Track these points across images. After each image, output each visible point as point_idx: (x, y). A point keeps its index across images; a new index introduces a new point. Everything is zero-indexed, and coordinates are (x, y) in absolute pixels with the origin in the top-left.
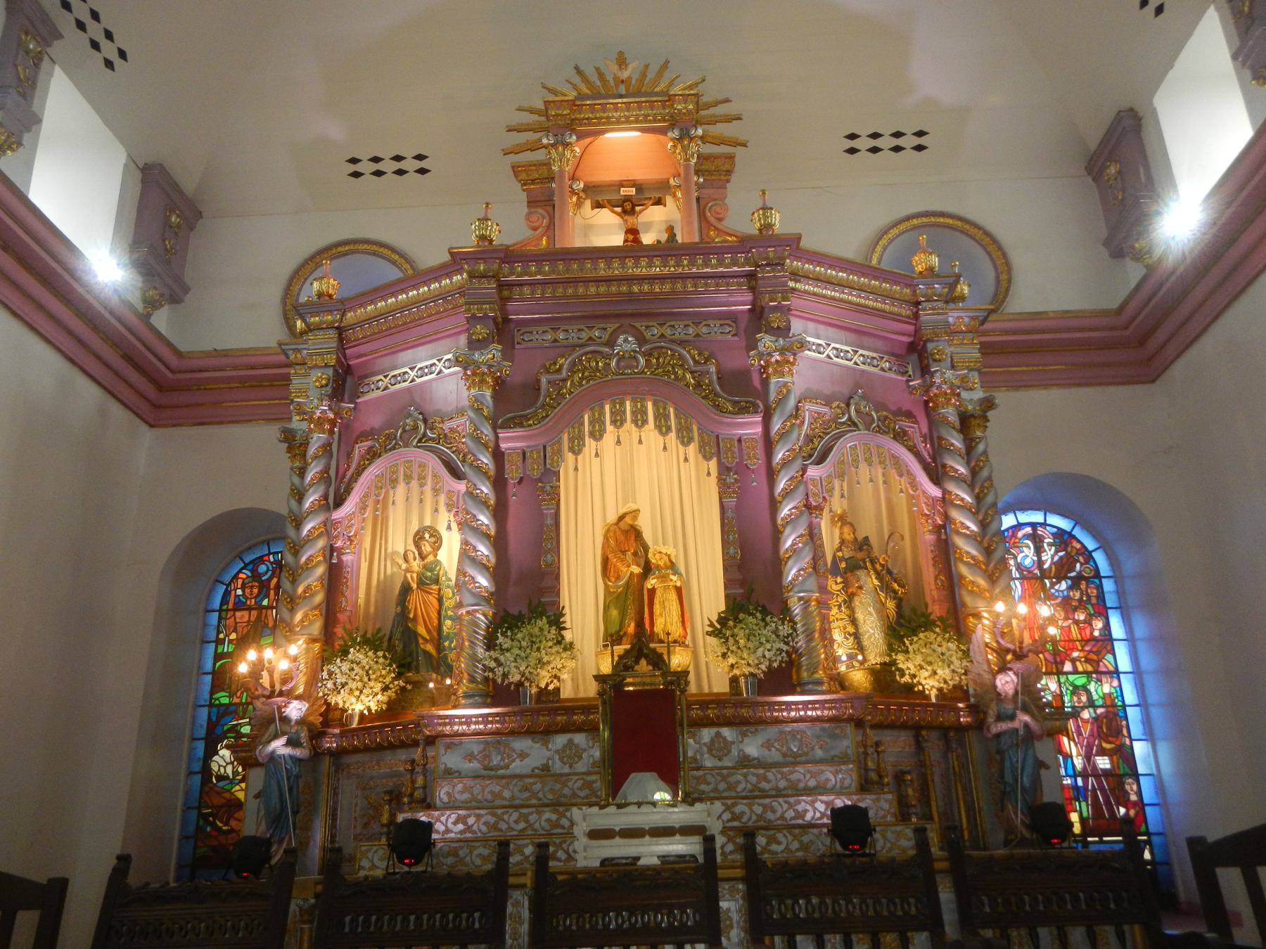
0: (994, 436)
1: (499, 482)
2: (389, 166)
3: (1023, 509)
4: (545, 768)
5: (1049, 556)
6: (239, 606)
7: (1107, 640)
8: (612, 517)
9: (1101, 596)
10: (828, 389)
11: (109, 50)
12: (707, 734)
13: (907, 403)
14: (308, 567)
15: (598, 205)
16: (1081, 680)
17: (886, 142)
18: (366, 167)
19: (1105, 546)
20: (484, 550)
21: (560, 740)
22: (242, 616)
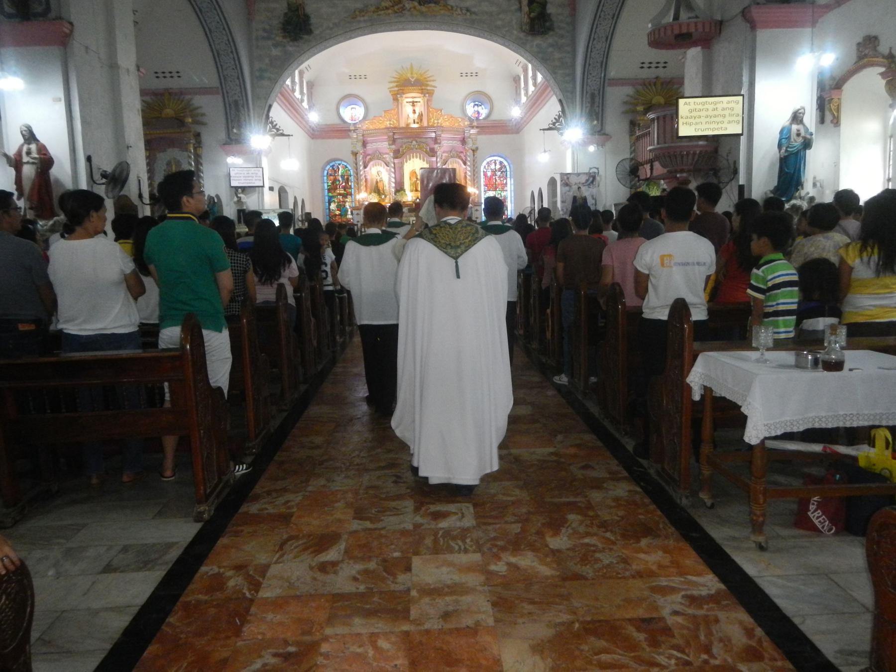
0: (478, 154)
1: (394, 168)
5: (498, 166)
6: (331, 175)
7: (506, 183)
9: (506, 176)
10: (447, 150)
11: (308, 69)
13: (461, 150)
14: (362, 179)
15: (407, 102)
16: (499, 192)
18: (353, 77)
19: (509, 164)
20: (393, 180)
22: (332, 177)
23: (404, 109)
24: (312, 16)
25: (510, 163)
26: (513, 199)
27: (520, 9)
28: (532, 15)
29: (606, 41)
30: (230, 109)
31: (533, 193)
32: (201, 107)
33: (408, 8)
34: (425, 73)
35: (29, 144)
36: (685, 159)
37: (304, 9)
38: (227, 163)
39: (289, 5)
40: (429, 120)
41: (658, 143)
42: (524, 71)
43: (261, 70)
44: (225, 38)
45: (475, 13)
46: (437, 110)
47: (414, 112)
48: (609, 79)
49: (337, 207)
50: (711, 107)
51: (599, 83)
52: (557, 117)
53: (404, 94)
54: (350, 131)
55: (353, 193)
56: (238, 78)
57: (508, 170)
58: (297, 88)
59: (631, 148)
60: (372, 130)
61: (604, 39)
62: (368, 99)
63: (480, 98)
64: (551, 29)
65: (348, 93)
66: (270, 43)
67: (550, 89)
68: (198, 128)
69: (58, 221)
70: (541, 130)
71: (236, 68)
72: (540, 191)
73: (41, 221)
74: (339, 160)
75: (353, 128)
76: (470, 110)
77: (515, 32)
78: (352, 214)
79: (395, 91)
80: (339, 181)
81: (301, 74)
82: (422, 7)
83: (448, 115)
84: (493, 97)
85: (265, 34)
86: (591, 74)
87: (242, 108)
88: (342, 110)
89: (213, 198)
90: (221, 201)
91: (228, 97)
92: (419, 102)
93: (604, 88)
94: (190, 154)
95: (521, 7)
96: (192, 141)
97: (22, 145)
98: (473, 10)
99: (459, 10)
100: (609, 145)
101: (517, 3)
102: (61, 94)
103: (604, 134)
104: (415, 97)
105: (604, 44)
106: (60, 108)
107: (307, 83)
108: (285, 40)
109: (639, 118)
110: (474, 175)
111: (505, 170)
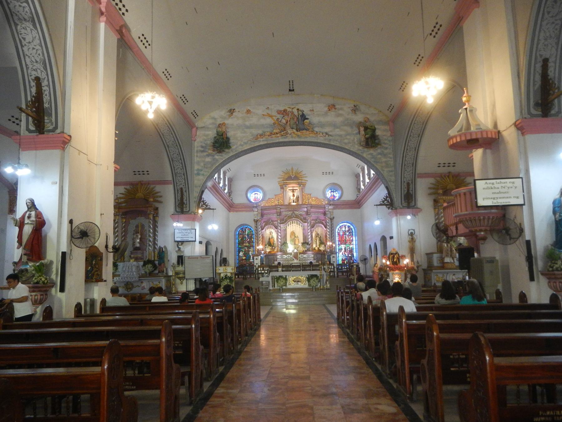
2: (259, 175)
3: (344, 222)
4: (286, 258)
5: (347, 229)
6: (241, 234)
7: (353, 240)
8: (291, 231)
9: (353, 235)
10: (314, 219)
12: (301, 255)
13: (323, 219)
15: (289, 190)
17: (328, 173)
18: (256, 175)
20: (280, 237)
21: (288, 255)
22: (241, 236)
23: (287, 194)
24: (231, 139)
25: (355, 227)
26: (357, 249)
27: (359, 132)
28: (367, 136)
29: (415, 150)
30: (178, 193)
31: (370, 245)
32: (160, 192)
33: (290, 133)
34: (301, 172)
35: (31, 211)
36: (482, 222)
37: (226, 134)
38: (173, 226)
39: (217, 132)
40: (303, 200)
41: (461, 211)
42: (362, 171)
43: (198, 170)
44: (177, 151)
45: (331, 135)
46: (308, 194)
47: (294, 195)
48: (418, 174)
49: (244, 254)
50: (499, 186)
51: (411, 176)
52: (385, 198)
53: (287, 185)
54: (254, 207)
55: (254, 245)
56: (184, 175)
57: (354, 231)
58: (222, 182)
59: (435, 217)
60: (267, 206)
61: (414, 150)
62: (266, 188)
63: (335, 187)
64: (378, 144)
65: (253, 184)
66: (205, 154)
67: (380, 180)
68: (157, 205)
69: (43, 263)
70: (375, 205)
71: (183, 169)
72: (375, 244)
73: (31, 263)
74: (246, 225)
75: (255, 206)
76: (329, 194)
77: (356, 146)
78: (253, 259)
79: (282, 183)
80: (246, 238)
81: (225, 173)
82: (298, 132)
83: (315, 197)
84: (343, 187)
85: (202, 149)
86: (406, 170)
87: (185, 194)
88: (249, 195)
89: (163, 248)
90: (167, 250)
91: (177, 185)
92: (297, 190)
93: (415, 180)
94: (151, 221)
95: (360, 132)
96: (152, 212)
97: (26, 212)
98: (330, 133)
99: (321, 133)
100: (420, 214)
101: (357, 129)
102: (58, 180)
103: (417, 208)
104: (294, 187)
105: (414, 153)
106: (56, 188)
107: (228, 179)
108: (213, 153)
109: (439, 198)
110: (332, 234)
111: (351, 231)
